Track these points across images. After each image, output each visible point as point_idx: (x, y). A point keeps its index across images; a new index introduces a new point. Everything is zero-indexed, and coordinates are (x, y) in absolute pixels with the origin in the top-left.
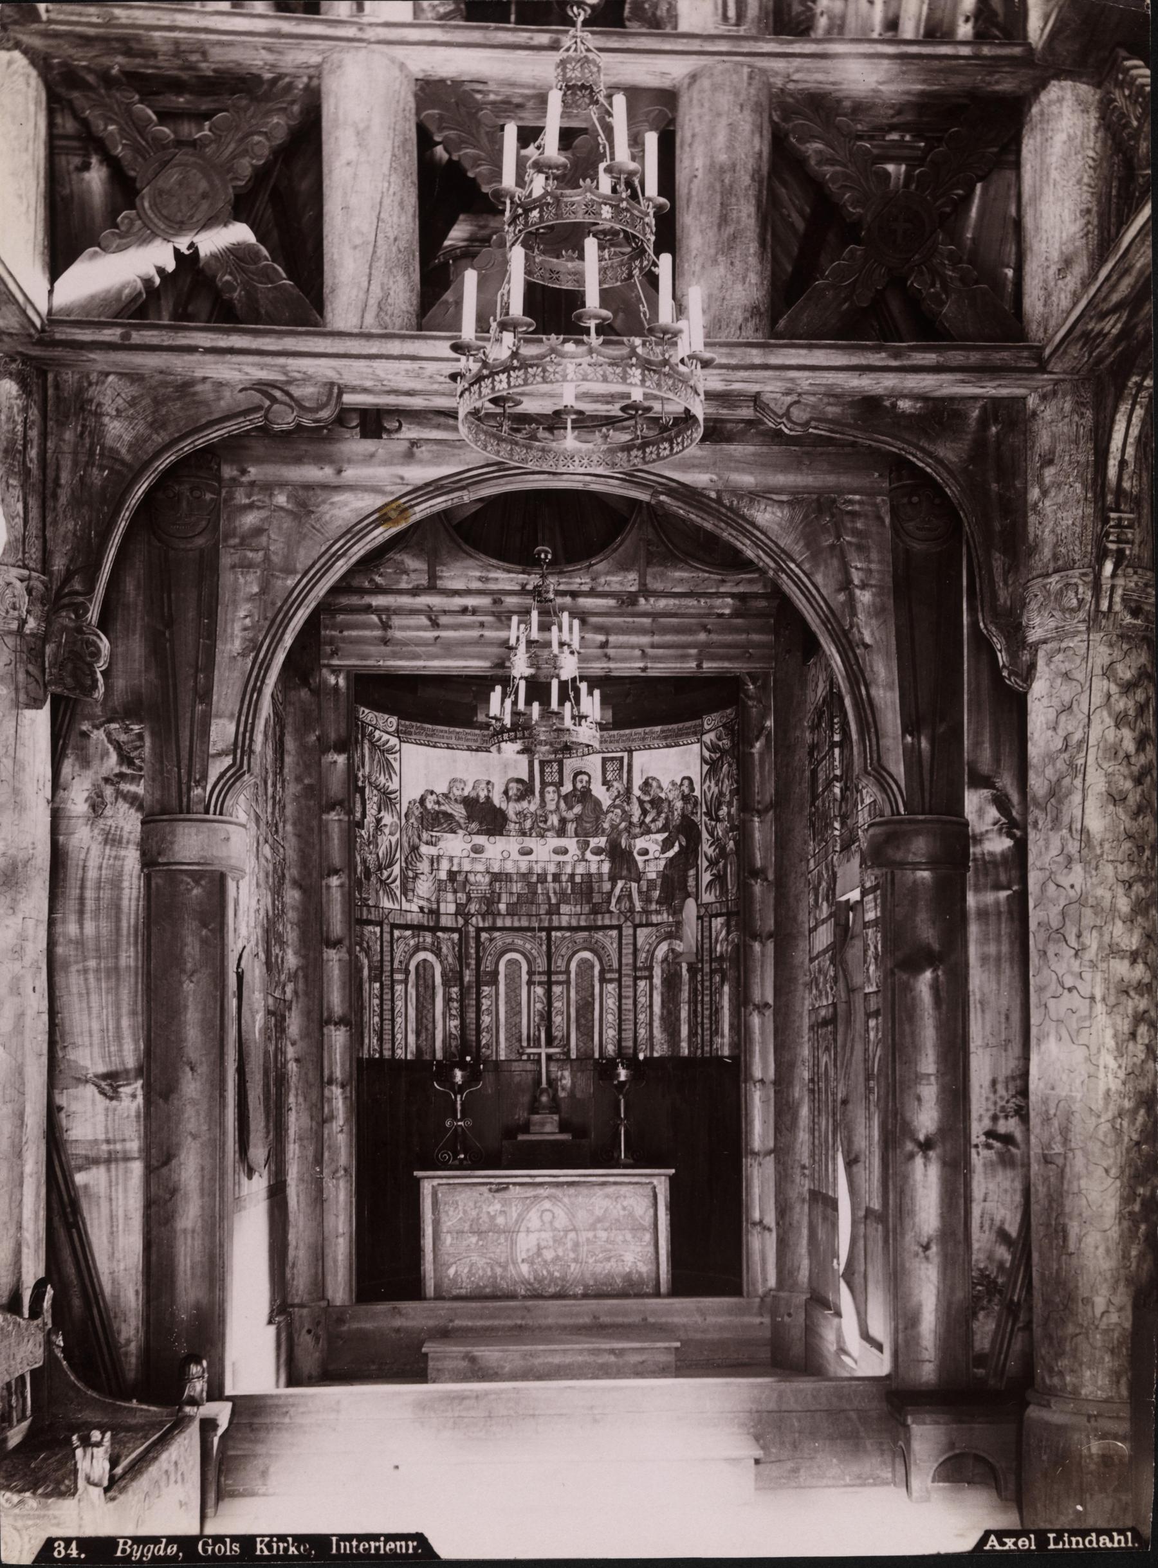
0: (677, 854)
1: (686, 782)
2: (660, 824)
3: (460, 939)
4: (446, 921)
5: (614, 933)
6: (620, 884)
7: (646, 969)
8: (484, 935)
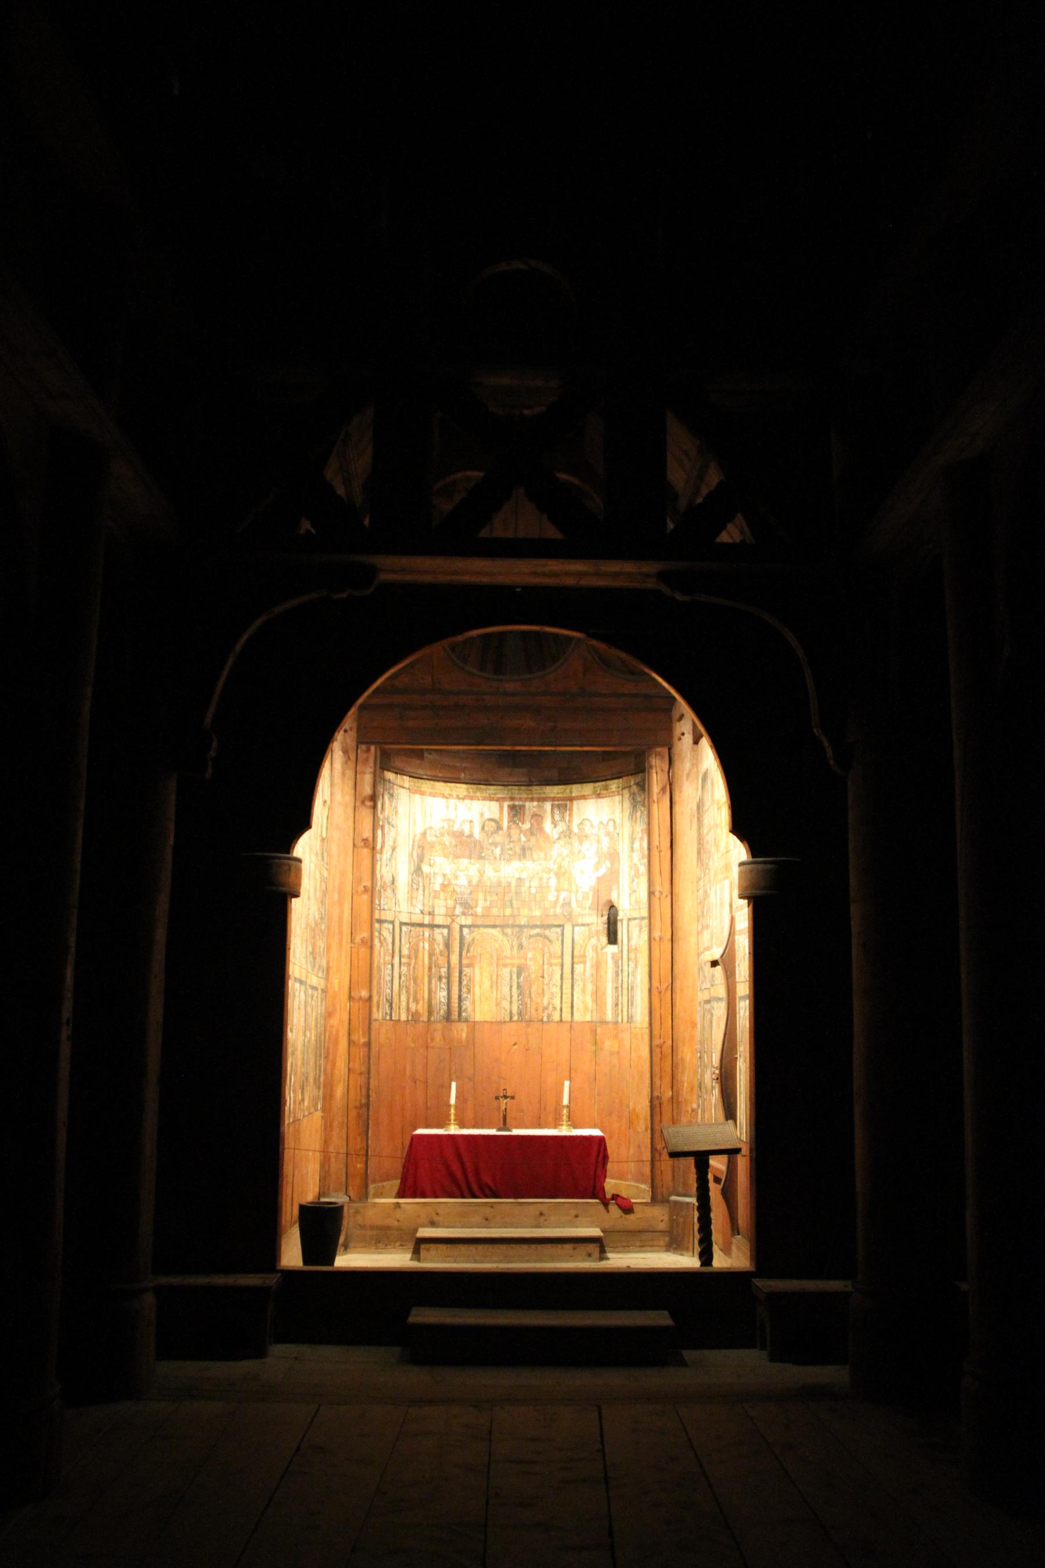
1: (611, 823)
3: (449, 933)
4: (438, 921)
5: (559, 930)
6: (563, 894)
7: (580, 956)
8: (466, 931)
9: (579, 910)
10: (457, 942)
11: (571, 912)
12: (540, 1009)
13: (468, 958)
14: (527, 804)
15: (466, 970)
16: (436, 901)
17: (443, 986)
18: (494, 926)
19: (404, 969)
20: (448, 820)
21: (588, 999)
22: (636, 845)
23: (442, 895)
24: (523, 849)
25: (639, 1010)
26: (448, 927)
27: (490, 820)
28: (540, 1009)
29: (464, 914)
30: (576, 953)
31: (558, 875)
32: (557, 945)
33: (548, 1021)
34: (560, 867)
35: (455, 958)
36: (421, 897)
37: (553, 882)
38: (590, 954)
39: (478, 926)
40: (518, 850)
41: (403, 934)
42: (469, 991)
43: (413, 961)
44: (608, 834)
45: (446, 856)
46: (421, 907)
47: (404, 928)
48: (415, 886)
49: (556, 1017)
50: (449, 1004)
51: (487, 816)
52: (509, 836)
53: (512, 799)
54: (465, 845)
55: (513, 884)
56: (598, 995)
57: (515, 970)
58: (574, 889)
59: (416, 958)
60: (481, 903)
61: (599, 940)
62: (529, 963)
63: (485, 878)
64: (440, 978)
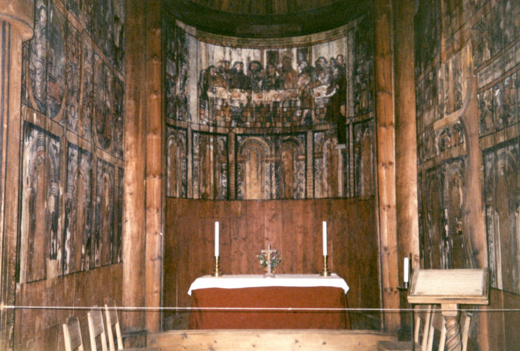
0: (335, 95)
1: (339, 58)
2: (326, 80)
3: (227, 139)
4: (220, 130)
5: (303, 136)
6: (306, 111)
8: (239, 138)
9: (318, 121)
10: (233, 145)
11: (312, 123)
12: (292, 191)
13: (241, 156)
14: (280, 51)
15: (240, 165)
16: (219, 118)
17: (224, 175)
18: (258, 135)
19: (196, 163)
20: (225, 62)
21: (325, 181)
22: (359, 70)
23: (222, 114)
24: (277, 81)
25: (363, 188)
26: (227, 135)
27: (255, 62)
28: (292, 191)
29: (238, 126)
30: (316, 151)
31: (302, 99)
32: (302, 146)
33: (298, 199)
34: (303, 92)
35: (231, 157)
36: (207, 114)
37: (299, 104)
38: (326, 151)
39: (248, 135)
40: (274, 82)
41: (194, 138)
42: (242, 180)
43: (202, 158)
44: (337, 66)
45: (225, 88)
46: (207, 120)
47: (195, 135)
48: (202, 106)
49: (303, 196)
50: (228, 188)
51: (252, 59)
52: (268, 73)
53: (270, 47)
54: (236, 79)
55: (271, 106)
56: (332, 181)
57: (273, 164)
58: (313, 107)
59: (205, 156)
60: (249, 119)
61: (331, 141)
62: (283, 160)
63: (252, 102)
64: (222, 172)
